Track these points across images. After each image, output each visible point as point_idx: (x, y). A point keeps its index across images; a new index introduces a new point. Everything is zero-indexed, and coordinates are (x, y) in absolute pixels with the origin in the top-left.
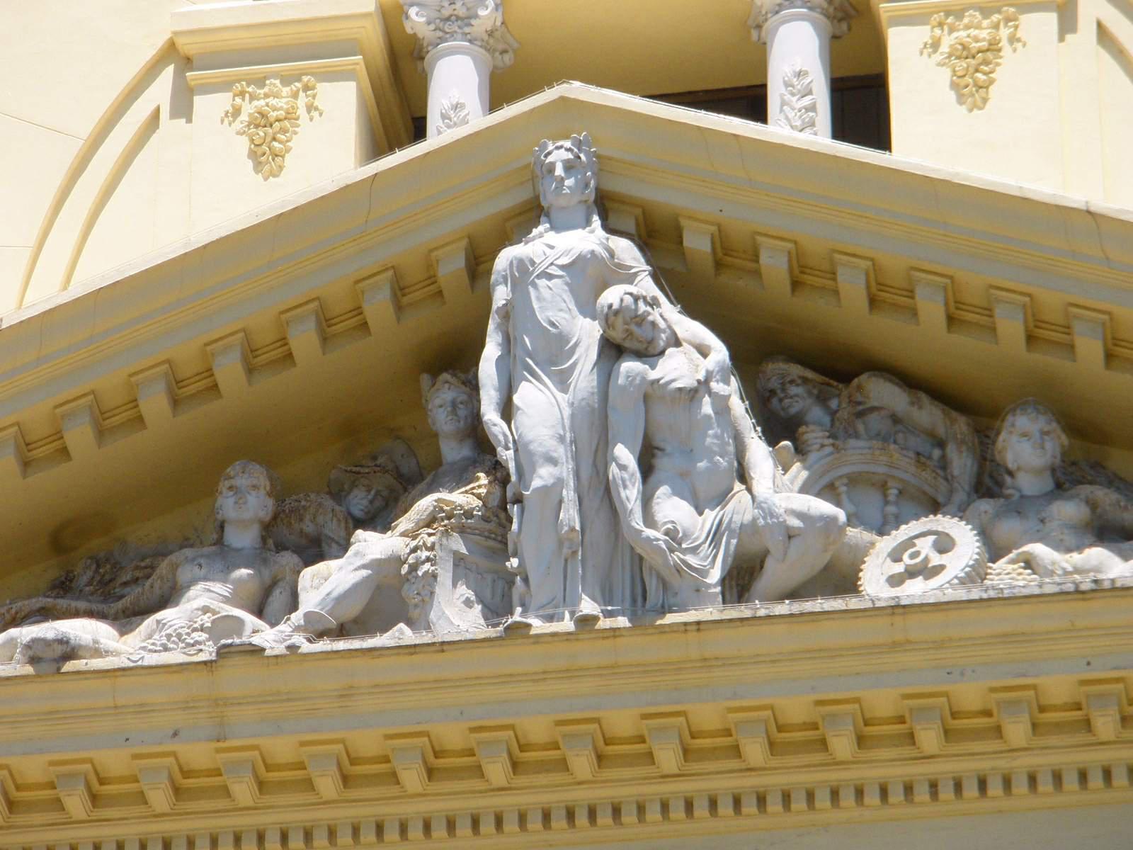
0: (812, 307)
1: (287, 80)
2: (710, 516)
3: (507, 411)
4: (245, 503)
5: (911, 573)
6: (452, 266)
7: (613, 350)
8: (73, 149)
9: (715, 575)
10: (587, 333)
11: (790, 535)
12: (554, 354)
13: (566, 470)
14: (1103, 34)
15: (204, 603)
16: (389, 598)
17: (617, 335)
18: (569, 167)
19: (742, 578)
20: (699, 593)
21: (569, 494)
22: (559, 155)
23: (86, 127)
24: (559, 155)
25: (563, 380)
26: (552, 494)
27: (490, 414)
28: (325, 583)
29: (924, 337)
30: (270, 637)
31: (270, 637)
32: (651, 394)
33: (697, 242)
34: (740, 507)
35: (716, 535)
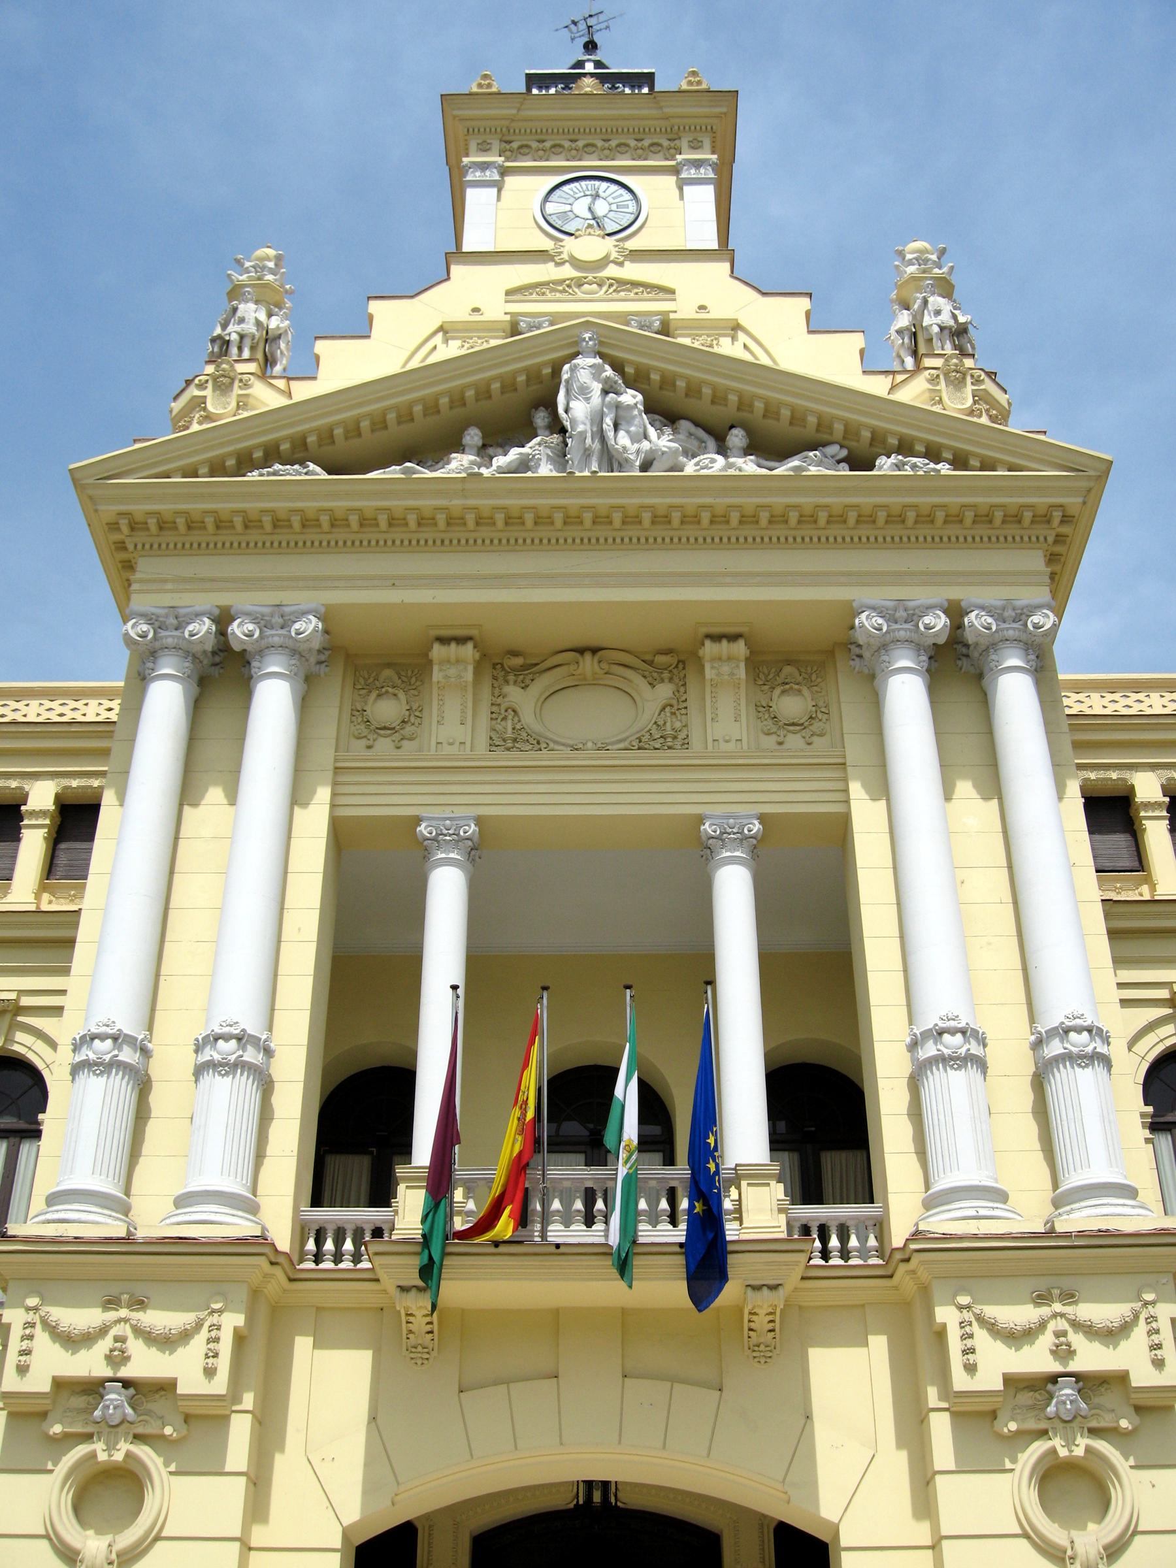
0: (667, 394)
1: (479, 338)
2: (636, 446)
3: (566, 411)
4: (473, 437)
5: (702, 468)
6: (547, 371)
7: (605, 392)
8: (408, 353)
9: (638, 463)
10: (597, 387)
11: (663, 453)
12: (584, 392)
13: (588, 427)
14: (745, 346)
15: (459, 464)
16: (525, 464)
17: (607, 388)
18: (590, 339)
19: (645, 467)
20: (632, 468)
21: (589, 435)
22: (587, 336)
23: (412, 348)
24: (587, 336)
25: (588, 400)
26: (582, 435)
27: (561, 410)
28: (500, 461)
29: (703, 407)
30: (485, 472)
31: (485, 472)
32: (618, 406)
33: (629, 370)
34: (646, 445)
35: (638, 451)
